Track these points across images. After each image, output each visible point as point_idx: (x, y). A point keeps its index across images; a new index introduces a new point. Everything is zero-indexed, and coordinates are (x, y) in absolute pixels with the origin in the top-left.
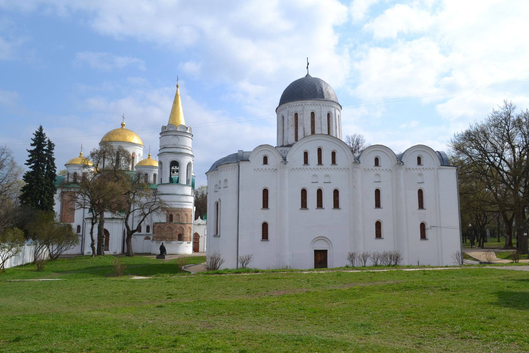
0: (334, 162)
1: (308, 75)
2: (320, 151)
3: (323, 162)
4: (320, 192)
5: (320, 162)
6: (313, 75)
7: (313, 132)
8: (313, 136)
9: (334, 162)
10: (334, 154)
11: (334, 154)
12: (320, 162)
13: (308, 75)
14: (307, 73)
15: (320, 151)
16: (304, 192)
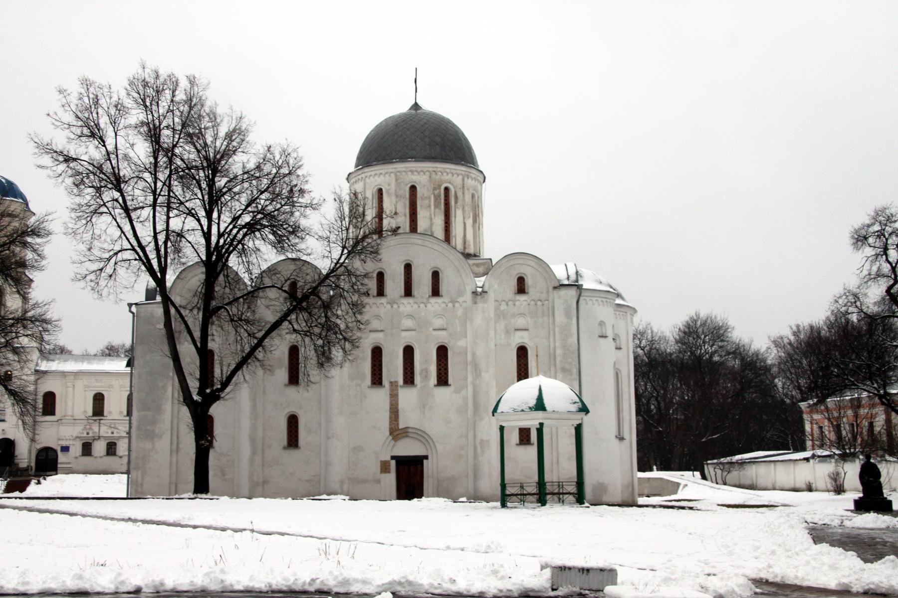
0: (436, 292)
1: (416, 106)
2: (408, 267)
3: (415, 291)
4: (409, 352)
5: (408, 292)
6: (429, 105)
7: (413, 228)
8: (414, 236)
9: (436, 292)
10: (436, 275)
11: (436, 275)
12: (408, 292)
13: (416, 106)
14: (413, 102)
15: (408, 267)
16: (377, 353)
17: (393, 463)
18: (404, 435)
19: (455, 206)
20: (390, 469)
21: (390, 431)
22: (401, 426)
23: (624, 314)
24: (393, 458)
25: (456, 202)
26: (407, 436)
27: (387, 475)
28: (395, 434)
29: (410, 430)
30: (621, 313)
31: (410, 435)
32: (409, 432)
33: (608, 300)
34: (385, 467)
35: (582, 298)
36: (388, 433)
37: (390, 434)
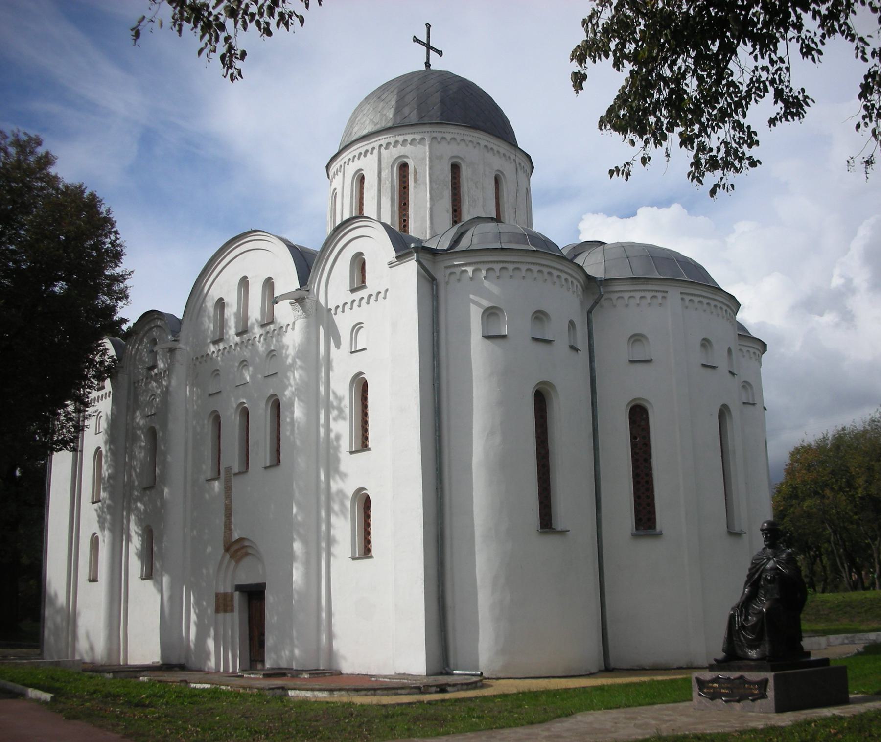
17: (237, 595)
18: (244, 551)
19: (414, 187)
20: (233, 606)
21: (224, 546)
22: (236, 536)
23: (659, 295)
24: (239, 588)
25: (416, 180)
26: (247, 554)
27: (228, 615)
28: (233, 549)
29: (246, 543)
30: (649, 295)
31: (250, 551)
32: (247, 546)
33: (511, 267)
34: (223, 604)
35: (440, 274)
36: (223, 551)
37: (227, 550)
